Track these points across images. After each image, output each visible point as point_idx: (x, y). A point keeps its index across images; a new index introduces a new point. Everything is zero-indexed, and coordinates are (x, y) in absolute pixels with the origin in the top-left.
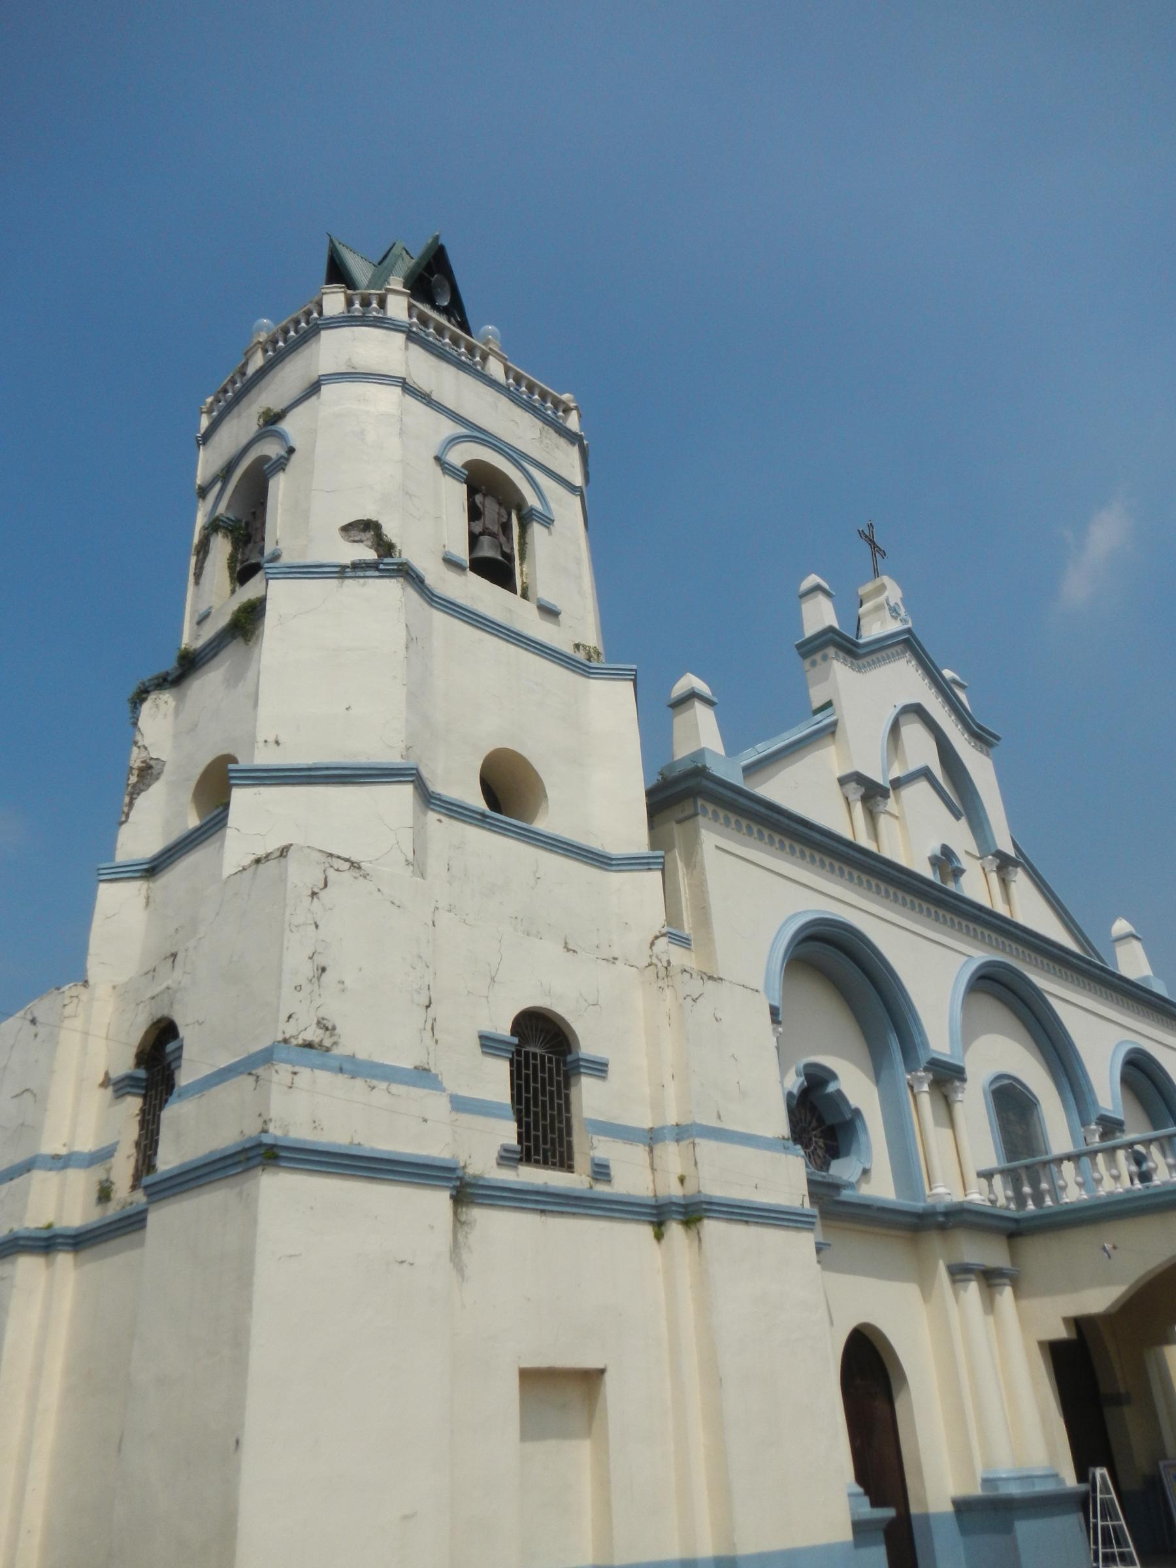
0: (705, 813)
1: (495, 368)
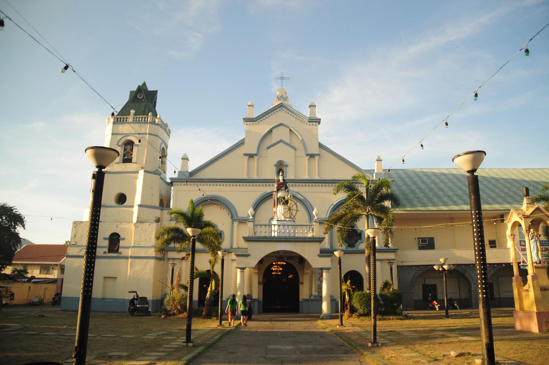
1: (131, 119)
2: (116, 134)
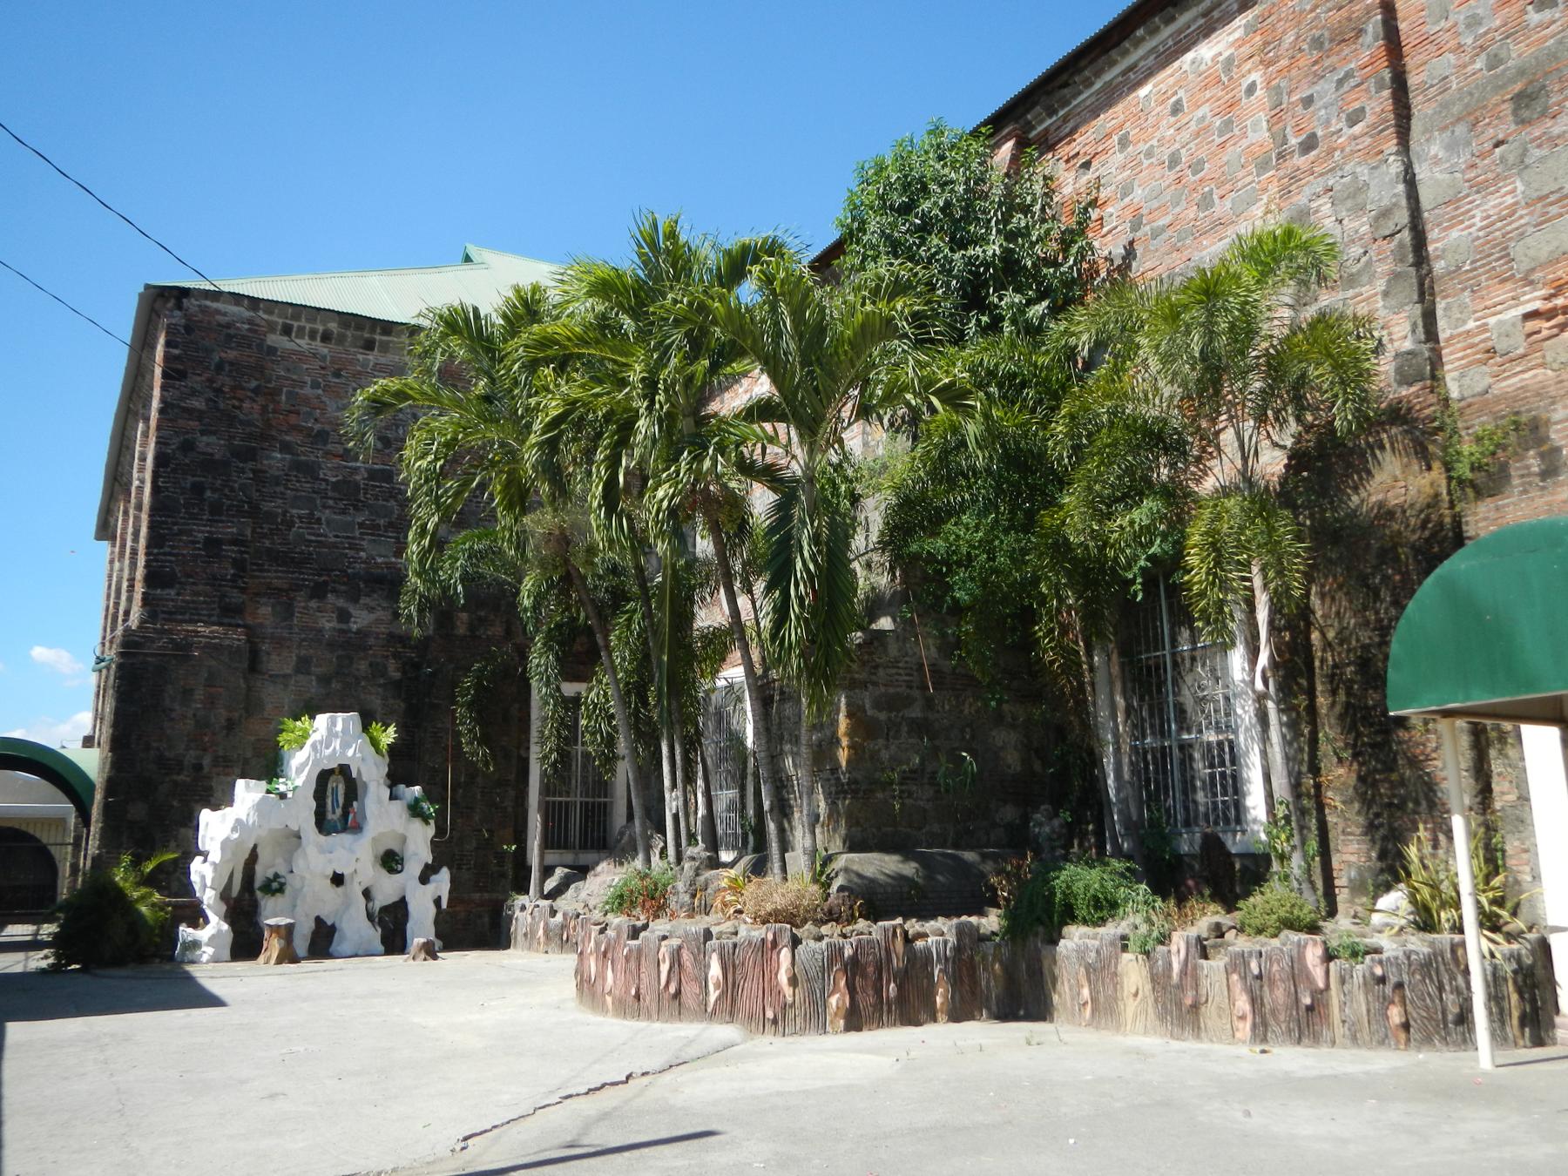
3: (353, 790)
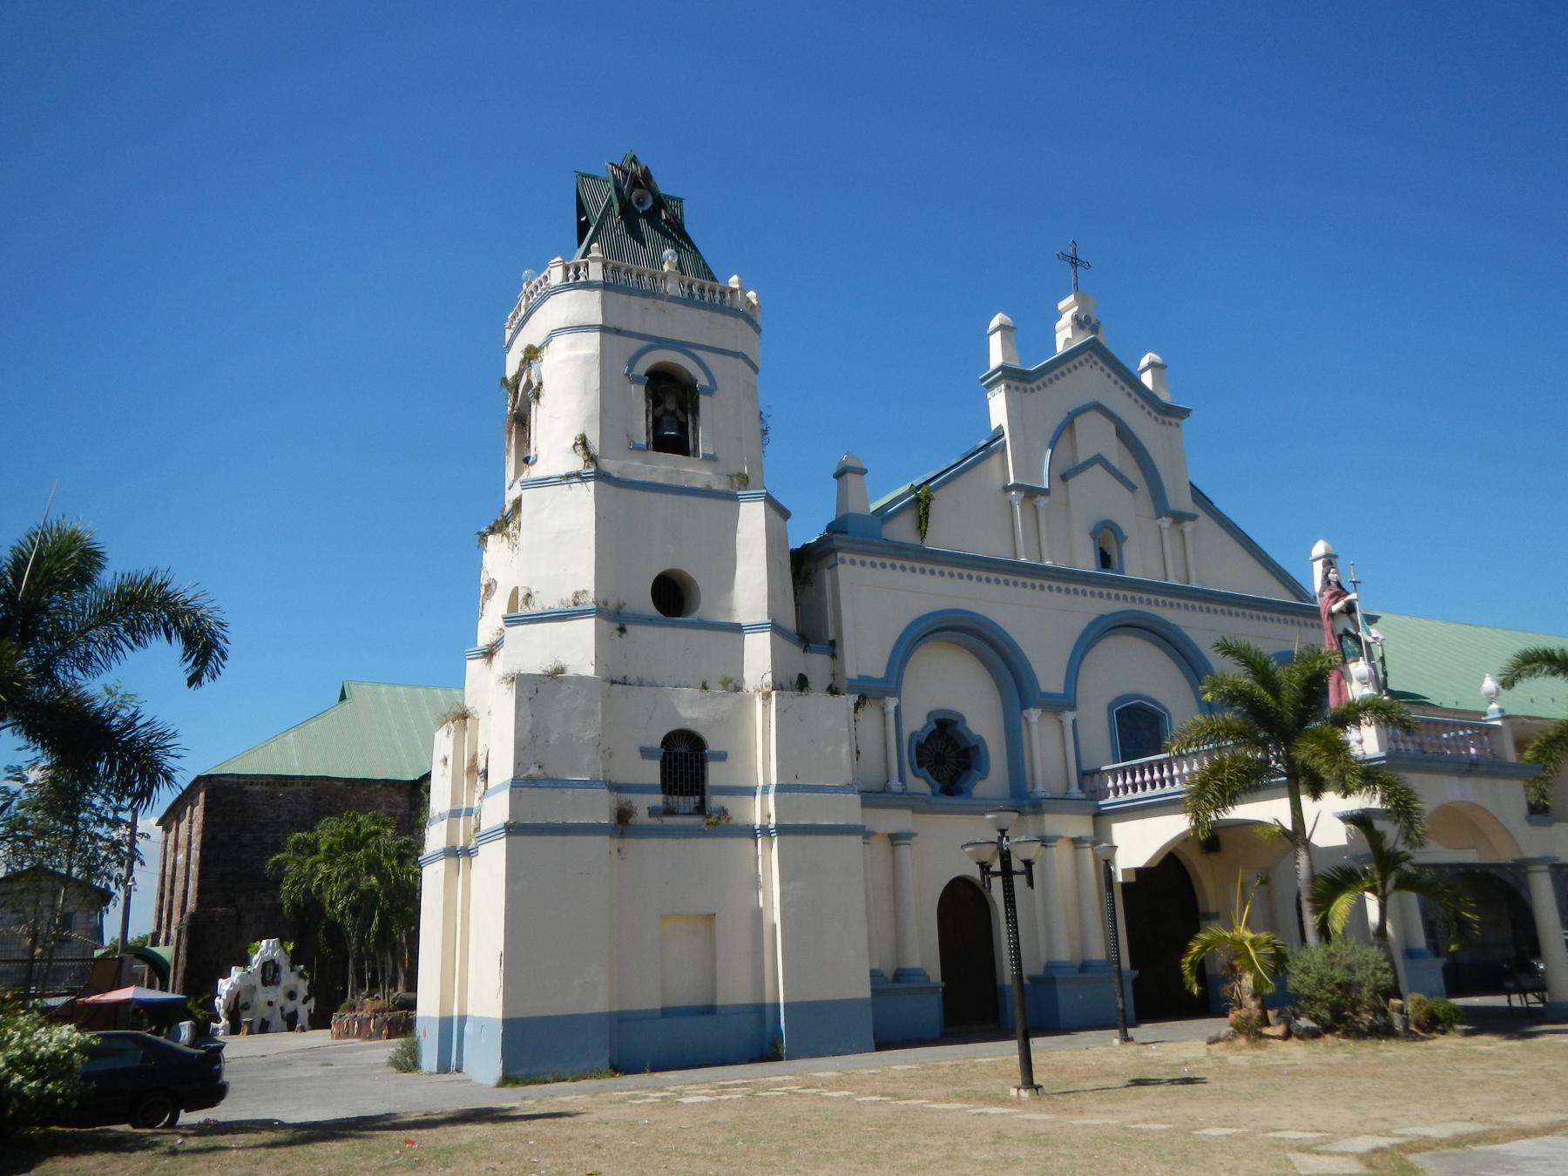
0: (843, 561)
2: (618, 332)
3: (277, 968)
